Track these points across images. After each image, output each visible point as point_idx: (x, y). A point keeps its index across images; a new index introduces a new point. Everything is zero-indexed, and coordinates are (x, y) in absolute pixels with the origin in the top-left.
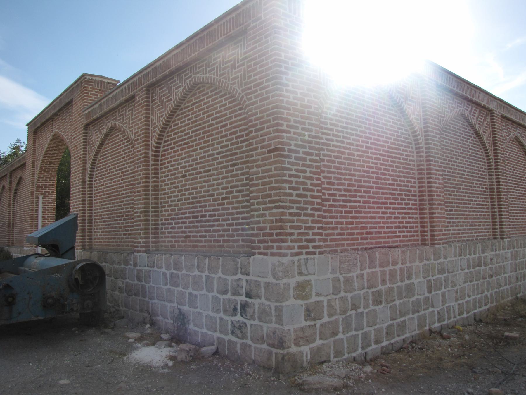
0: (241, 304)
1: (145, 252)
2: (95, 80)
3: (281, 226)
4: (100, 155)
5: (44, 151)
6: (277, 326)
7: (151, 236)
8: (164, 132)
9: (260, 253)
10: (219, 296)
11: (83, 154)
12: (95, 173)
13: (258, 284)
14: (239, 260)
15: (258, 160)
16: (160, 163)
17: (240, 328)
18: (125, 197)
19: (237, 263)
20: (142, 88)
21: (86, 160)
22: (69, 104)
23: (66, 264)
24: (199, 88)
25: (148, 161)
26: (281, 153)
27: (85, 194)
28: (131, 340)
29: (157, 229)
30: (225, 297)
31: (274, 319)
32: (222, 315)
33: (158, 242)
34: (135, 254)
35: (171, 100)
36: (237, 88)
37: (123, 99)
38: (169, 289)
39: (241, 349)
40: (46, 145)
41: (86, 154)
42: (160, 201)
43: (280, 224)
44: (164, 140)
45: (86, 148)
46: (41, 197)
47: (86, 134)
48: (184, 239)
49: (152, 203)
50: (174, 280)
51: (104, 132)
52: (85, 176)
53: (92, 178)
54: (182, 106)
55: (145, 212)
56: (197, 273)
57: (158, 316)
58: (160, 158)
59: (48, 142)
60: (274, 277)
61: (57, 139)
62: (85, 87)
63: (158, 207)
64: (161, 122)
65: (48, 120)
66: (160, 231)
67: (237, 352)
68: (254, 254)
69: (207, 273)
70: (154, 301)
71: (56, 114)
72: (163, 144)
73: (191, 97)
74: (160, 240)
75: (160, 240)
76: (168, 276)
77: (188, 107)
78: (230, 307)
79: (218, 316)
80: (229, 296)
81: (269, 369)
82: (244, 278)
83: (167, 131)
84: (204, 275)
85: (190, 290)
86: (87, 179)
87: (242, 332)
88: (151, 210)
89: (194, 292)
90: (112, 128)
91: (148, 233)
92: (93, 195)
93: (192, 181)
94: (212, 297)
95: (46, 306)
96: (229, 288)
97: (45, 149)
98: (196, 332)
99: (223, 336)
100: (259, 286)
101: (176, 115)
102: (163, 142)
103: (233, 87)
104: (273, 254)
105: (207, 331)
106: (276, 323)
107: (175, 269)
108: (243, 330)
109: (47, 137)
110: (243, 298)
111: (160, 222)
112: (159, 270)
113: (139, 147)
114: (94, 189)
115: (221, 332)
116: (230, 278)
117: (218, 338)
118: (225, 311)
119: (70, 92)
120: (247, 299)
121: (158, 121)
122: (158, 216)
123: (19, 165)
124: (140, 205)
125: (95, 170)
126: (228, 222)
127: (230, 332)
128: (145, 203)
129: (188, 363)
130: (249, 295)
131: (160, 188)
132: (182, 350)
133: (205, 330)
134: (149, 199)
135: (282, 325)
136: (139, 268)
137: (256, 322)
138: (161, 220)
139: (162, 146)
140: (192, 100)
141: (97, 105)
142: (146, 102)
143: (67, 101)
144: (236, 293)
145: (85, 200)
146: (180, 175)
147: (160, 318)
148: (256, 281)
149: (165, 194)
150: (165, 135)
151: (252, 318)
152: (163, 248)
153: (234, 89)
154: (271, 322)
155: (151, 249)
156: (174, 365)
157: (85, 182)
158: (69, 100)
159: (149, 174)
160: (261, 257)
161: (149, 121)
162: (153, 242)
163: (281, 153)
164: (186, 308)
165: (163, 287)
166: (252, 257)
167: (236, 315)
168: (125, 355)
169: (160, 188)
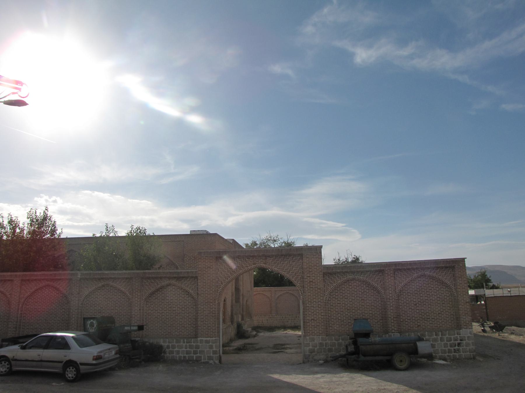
1: (399, 332)
13: (465, 337)
32: (449, 348)
56: (435, 337)
79: (447, 349)
80: (452, 342)
81: (471, 359)
82: (459, 336)
84: (439, 337)
110: (459, 341)
116: (452, 337)
118: (451, 346)
130: (461, 340)
133: (440, 354)
137: (465, 347)
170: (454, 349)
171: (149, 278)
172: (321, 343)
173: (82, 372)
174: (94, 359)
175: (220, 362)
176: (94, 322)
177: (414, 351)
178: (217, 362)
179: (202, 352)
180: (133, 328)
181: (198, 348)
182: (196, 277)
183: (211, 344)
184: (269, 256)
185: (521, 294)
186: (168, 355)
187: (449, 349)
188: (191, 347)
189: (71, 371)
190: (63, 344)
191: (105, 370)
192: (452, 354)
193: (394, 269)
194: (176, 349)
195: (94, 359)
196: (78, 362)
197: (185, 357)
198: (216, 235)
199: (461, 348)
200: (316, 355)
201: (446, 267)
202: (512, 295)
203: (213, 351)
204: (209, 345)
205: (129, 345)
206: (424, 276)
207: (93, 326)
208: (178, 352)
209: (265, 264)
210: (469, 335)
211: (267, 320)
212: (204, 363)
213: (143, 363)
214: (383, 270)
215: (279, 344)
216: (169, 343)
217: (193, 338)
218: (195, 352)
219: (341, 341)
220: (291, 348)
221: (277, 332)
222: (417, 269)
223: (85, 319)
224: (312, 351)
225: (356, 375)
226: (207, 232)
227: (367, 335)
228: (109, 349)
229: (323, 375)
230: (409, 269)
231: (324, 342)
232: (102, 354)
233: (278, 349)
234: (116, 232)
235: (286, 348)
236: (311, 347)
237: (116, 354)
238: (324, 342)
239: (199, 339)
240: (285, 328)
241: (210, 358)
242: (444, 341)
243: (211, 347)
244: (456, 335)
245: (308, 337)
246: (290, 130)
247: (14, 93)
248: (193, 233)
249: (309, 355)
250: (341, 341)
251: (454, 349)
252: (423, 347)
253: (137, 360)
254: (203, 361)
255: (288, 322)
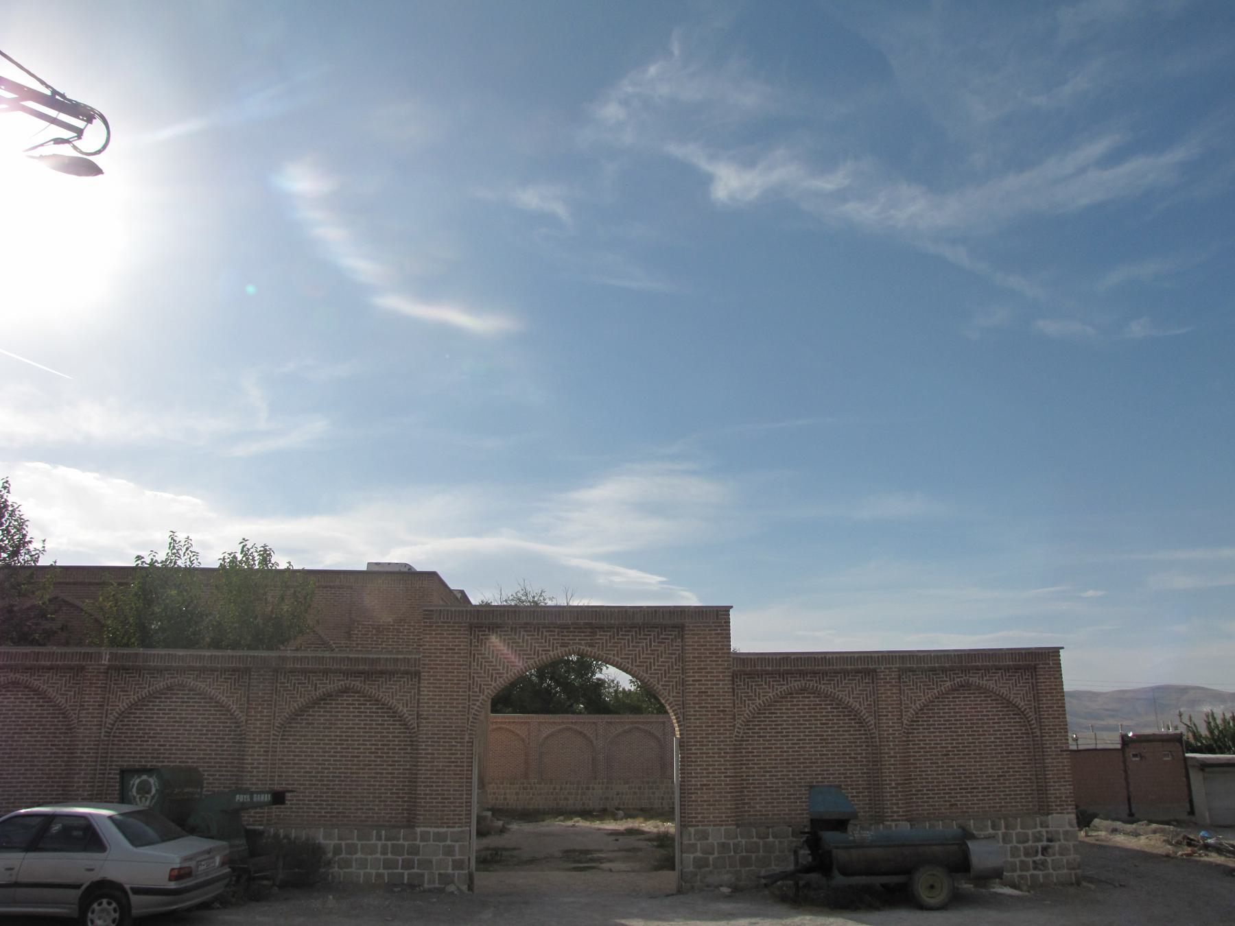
13: (1058, 833)
56: (991, 831)
79: (1017, 860)
80: (1030, 843)
81: (1072, 884)
82: (1044, 830)
110: (1045, 843)
116: (1030, 832)
118: (1027, 854)
130: (1050, 840)
137: (1057, 857)
144: (1039, 840)
170: (1034, 862)
171: (292, 671)
172: (723, 846)
173: (135, 912)
174: (170, 880)
175: (470, 888)
176: (152, 780)
177: (960, 865)
178: (465, 888)
179: (427, 864)
180: (256, 798)
181: (417, 854)
182: (417, 674)
183: (449, 842)
184: (601, 628)
185: (1099, 747)
186: (336, 869)
187: (1022, 862)
188: (397, 850)
189: (103, 910)
190: (85, 836)
191: (189, 909)
192: (1028, 874)
193: (899, 669)
194: (359, 855)
195: (170, 880)
196: (127, 887)
197: (379, 875)
198: (433, 575)
199: (1049, 859)
200: (711, 872)
201: (1017, 668)
202: (1081, 747)
203: (453, 861)
204: (445, 846)
205: (241, 842)
206: (966, 686)
207: (149, 792)
208: (363, 864)
209: (591, 646)
210: (1068, 828)
211: (517, 794)
212: (430, 891)
213: (275, 890)
214: (875, 671)
215: (574, 851)
216: (340, 838)
217: (403, 827)
218: (408, 865)
219: (771, 839)
220: (611, 861)
221: (545, 823)
222: (952, 669)
223: (126, 773)
224: (701, 864)
225: (832, 920)
226: (410, 568)
227: (840, 824)
228: (209, 852)
229: (753, 920)
230: (933, 670)
231: (731, 842)
232: (192, 864)
233: (580, 862)
234: (196, 554)
235: (600, 860)
236: (699, 854)
237: (223, 864)
238: (731, 842)
239: (418, 830)
240: (569, 814)
241: (446, 879)
242: (1011, 842)
243: (449, 851)
244: (1039, 829)
245: (692, 830)
246: (653, 326)
247: (59, 141)
248: (376, 569)
249: (695, 874)
250: (771, 839)
251: (1034, 862)
252: (982, 854)
253: (265, 882)
254: (426, 886)
255: (566, 799)
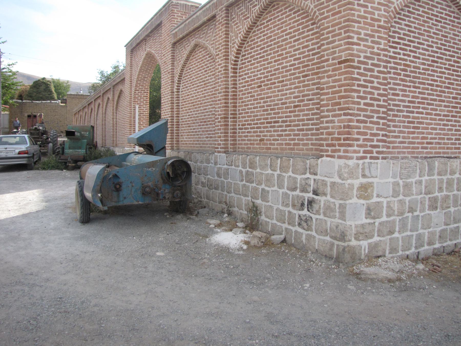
0: (308, 200)
1: (225, 152)
2: (181, 4)
3: (348, 131)
4: (185, 69)
5: (139, 68)
6: (340, 221)
7: (230, 139)
8: (242, 47)
9: (327, 156)
10: (289, 192)
11: (172, 69)
12: (181, 85)
13: (324, 183)
14: (308, 162)
15: (329, 71)
16: (238, 75)
17: (306, 221)
18: (207, 106)
19: (307, 163)
20: (222, 8)
21: (174, 74)
22: (159, 26)
23: (159, 160)
24: (274, 6)
25: (228, 74)
26: (351, 64)
27: (173, 103)
28: (212, 226)
29: (235, 133)
30: (294, 193)
31: (337, 214)
32: (290, 209)
33: (236, 144)
34: (216, 154)
35: (248, 18)
36: (309, 4)
37: (205, 19)
38: (245, 185)
39: (306, 239)
40: (141, 63)
41: (174, 69)
42: (238, 108)
43: (347, 130)
44: (242, 54)
45: (173, 64)
46: (137, 106)
47: (173, 52)
48: (258, 142)
49: (231, 110)
50: (249, 178)
51: (189, 49)
52: (174, 87)
53: (179, 89)
54: (258, 23)
55: (225, 118)
56: (269, 171)
57: (234, 207)
58: (238, 71)
59: (142, 59)
60: (340, 177)
61: (150, 57)
62: (172, 10)
63: (236, 114)
64: (239, 39)
65: (142, 41)
66: (237, 135)
67: (302, 241)
68: (322, 156)
69: (278, 172)
70: (231, 195)
71: (148, 36)
72: (241, 58)
73: (267, 14)
74: (238, 142)
75: (238, 142)
76: (244, 173)
77: (264, 23)
78: (298, 202)
79: (287, 209)
80: (297, 192)
81: (331, 258)
82: (312, 177)
83: (244, 46)
84: (276, 174)
85: (263, 186)
86: (175, 90)
87: (307, 225)
88: (230, 116)
89: (267, 188)
90: (196, 45)
91: (227, 136)
92: (180, 104)
93: (267, 91)
94: (283, 193)
95: (144, 194)
96: (298, 185)
97: (140, 66)
98: (267, 223)
99: (290, 227)
100: (326, 185)
101: (252, 31)
102: (240, 56)
103: (306, 3)
104: (340, 157)
105: (276, 222)
106: (339, 218)
107: (250, 168)
108: (309, 223)
109: (141, 55)
110: (311, 195)
111: (238, 127)
112: (236, 168)
113: (220, 60)
114: (180, 99)
115: (289, 224)
116: (299, 177)
117: (286, 229)
118: (294, 206)
119: (160, 15)
120: (315, 197)
121: (237, 38)
122: (236, 122)
123: (120, 80)
124: (220, 112)
125: (182, 82)
126: (299, 128)
127: (297, 224)
128: (225, 110)
129: (260, 248)
130: (315, 193)
131: (238, 97)
132: (254, 237)
133: (274, 221)
134: (228, 107)
135: (345, 221)
136: (218, 166)
137: (321, 217)
138: (239, 125)
139: (240, 60)
140: (267, 18)
141: (183, 25)
142: (226, 20)
143: (157, 24)
144: (304, 190)
145: (173, 108)
146: (256, 86)
147: (236, 209)
148: (323, 181)
149: (242, 102)
150: (243, 50)
151: (318, 213)
152: (240, 150)
153: (307, 5)
154: (335, 217)
155: (230, 150)
156: (248, 249)
157: (174, 92)
158: (159, 22)
159: (228, 85)
160: (329, 159)
161: (228, 38)
162: (231, 144)
163: (351, 64)
164: (259, 202)
165: (239, 183)
166: (320, 159)
167: (303, 210)
168: (207, 237)
169: (238, 97)
192: (293, 229)
210: (337, 179)
